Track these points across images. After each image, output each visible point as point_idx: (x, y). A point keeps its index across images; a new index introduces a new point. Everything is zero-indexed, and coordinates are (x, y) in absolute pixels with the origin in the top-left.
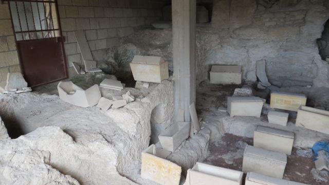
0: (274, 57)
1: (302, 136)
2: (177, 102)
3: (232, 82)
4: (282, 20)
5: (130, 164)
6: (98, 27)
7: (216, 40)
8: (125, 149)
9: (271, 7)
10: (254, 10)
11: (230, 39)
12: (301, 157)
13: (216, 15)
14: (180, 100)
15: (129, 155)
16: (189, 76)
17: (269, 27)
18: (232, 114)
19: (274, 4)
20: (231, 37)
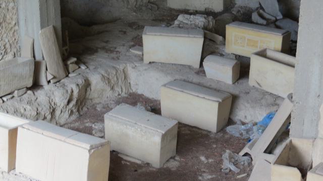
1: (248, 103)
2: (22, 23)
3: (207, 6)
12: (232, 137)
18: (147, 59)
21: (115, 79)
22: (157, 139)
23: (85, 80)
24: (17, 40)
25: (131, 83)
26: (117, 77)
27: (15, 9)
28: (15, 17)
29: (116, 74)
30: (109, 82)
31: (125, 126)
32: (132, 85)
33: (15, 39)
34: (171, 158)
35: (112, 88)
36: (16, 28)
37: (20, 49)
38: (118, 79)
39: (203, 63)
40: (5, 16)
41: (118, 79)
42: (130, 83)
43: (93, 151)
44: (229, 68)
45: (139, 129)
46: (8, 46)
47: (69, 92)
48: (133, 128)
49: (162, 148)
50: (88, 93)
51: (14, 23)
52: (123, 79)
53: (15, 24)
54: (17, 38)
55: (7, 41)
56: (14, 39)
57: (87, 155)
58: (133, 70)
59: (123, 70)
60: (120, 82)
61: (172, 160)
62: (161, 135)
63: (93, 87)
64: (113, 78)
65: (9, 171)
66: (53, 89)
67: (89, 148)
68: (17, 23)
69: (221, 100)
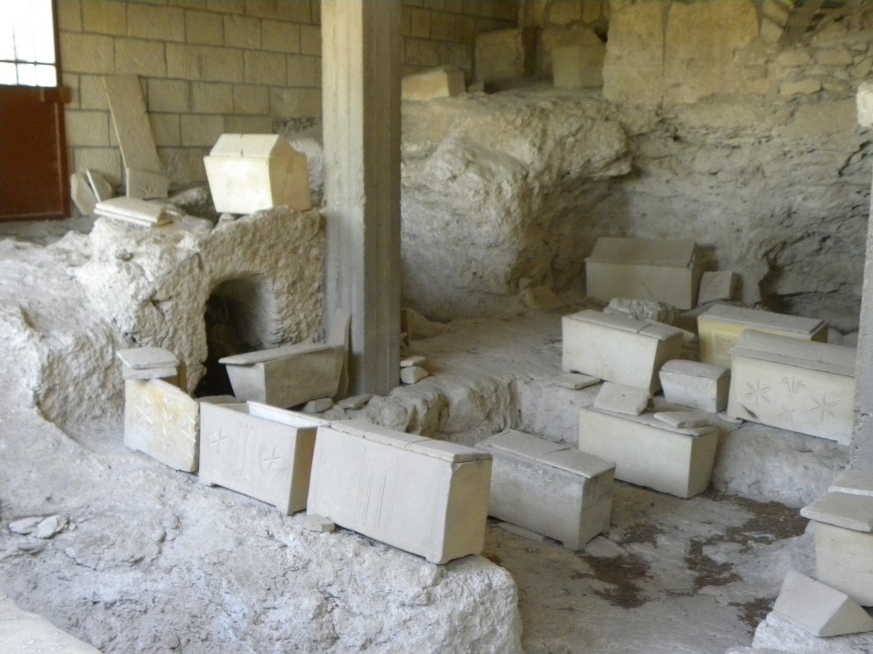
0: (823, 214)
2: (331, 285)
4: (840, 75)
5: (98, 412)
6: (194, 75)
7: (609, 145)
8: (82, 360)
9: (810, 29)
10: (747, 38)
11: (671, 143)
13: (619, 58)
14: (339, 281)
15: (95, 380)
16: (363, 201)
17: (795, 100)
19: (818, 17)
20: (676, 138)
21: (494, 399)
22: (576, 490)
23: (439, 396)
24: (319, 318)
25: (522, 410)
26: (497, 396)
27: (322, 260)
28: (318, 275)
29: (496, 390)
30: (483, 404)
31: (514, 465)
32: (524, 416)
33: (317, 316)
34: (601, 534)
35: (488, 417)
36: (320, 295)
37: (324, 333)
38: (498, 401)
39: (661, 374)
40: (302, 271)
41: (498, 401)
42: (520, 411)
43: (459, 465)
44: (711, 382)
45: (541, 472)
46: (303, 326)
47: (410, 411)
48: (528, 470)
49: (584, 509)
50: (443, 420)
51: (316, 285)
52: (508, 401)
53: (319, 287)
54: (320, 314)
55: (302, 316)
56: (314, 315)
57: (449, 472)
58: (527, 387)
59: (510, 384)
60: (502, 406)
61: (601, 538)
62: (583, 480)
63: (453, 411)
64: (490, 397)
65: (293, 513)
66: (380, 405)
67: (452, 460)
68: (322, 288)
69: (696, 434)
